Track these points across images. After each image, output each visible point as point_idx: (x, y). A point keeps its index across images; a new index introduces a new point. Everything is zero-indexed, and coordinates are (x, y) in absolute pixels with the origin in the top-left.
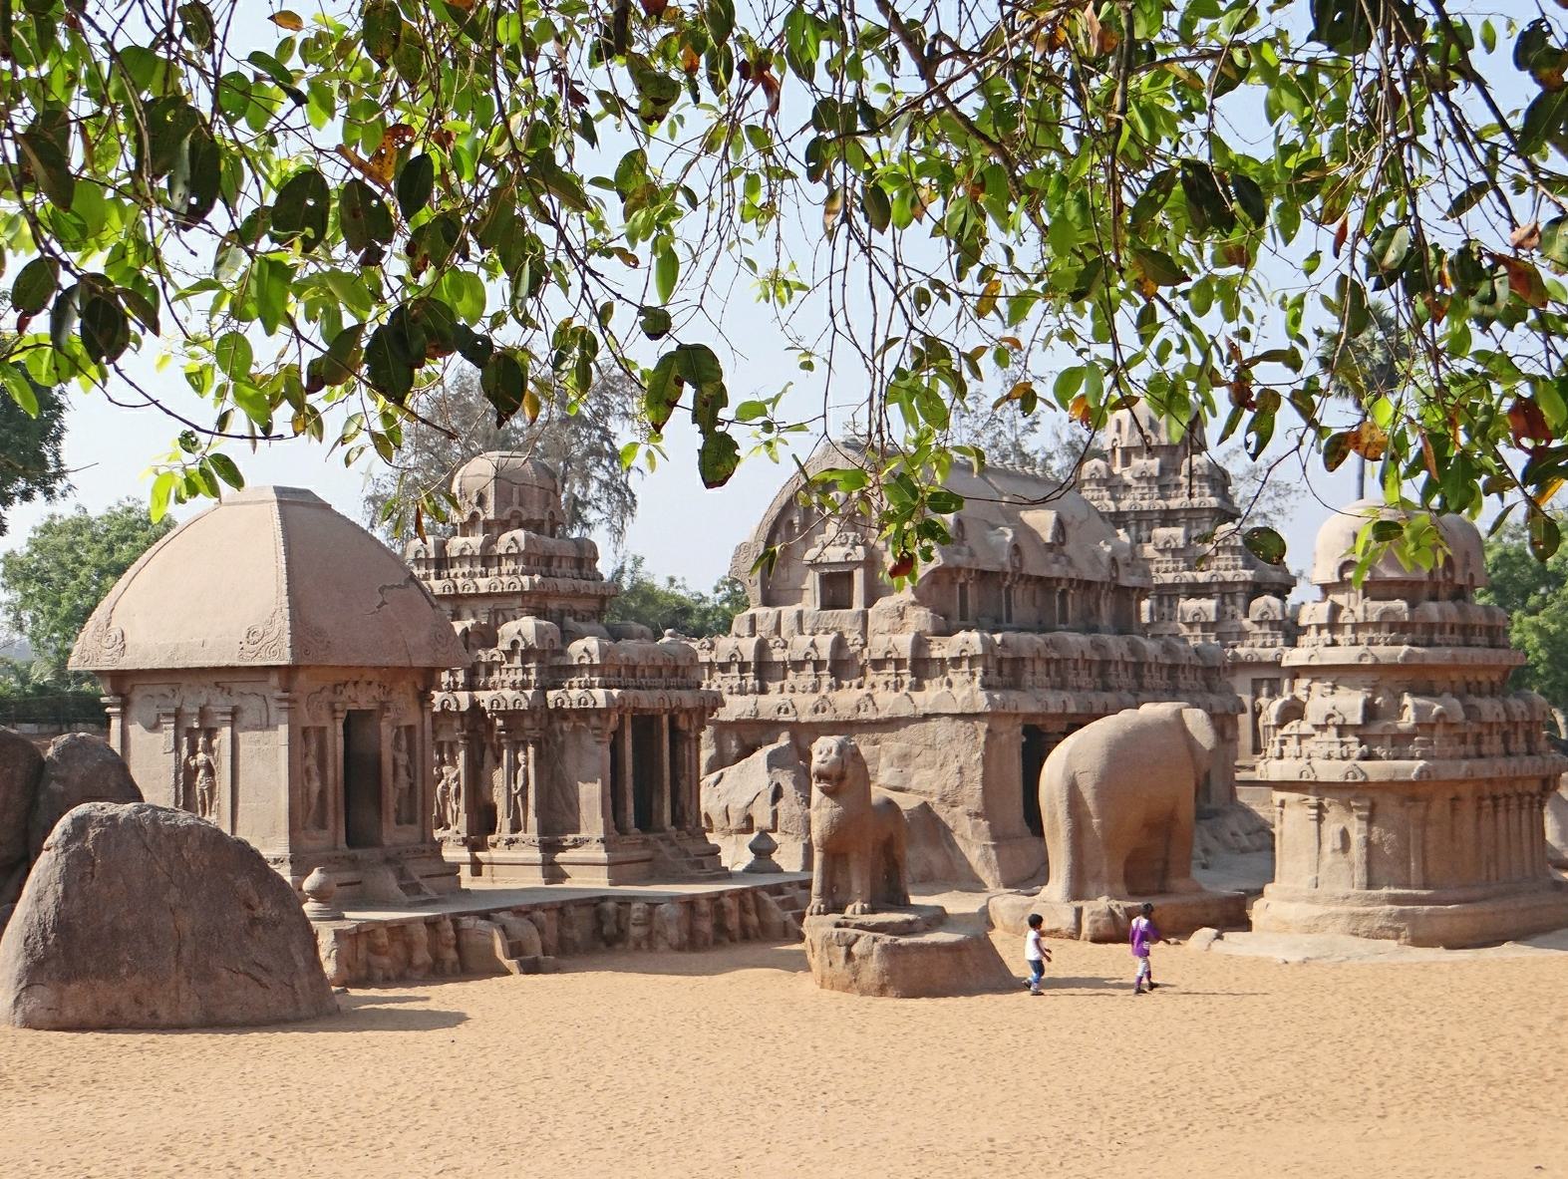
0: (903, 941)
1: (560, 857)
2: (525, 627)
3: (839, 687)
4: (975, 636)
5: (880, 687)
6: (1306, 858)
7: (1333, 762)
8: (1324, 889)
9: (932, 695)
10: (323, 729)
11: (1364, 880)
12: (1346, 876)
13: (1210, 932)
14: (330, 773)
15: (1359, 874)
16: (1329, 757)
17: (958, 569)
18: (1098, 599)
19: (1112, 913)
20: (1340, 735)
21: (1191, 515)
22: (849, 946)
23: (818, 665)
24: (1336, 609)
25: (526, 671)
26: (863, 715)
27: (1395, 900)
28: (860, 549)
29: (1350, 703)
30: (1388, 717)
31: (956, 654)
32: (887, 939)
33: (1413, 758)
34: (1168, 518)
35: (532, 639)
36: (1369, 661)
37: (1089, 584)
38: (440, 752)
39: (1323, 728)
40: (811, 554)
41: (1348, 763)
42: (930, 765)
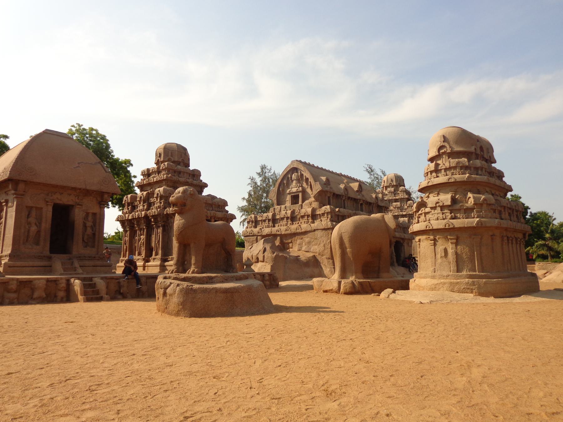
0: (196, 286)
1: (166, 263)
2: (160, 190)
3: (293, 224)
4: (328, 207)
5: (303, 223)
6: (430, 261)
7: (440, 221)
8: (437, 273)
9: (317, 224)
10: (42, 208)
11: (456, 268)
12: (447, 268)
13: (390, 290)
14: (43, 225)
15: (453, 267)
16: (438, 219)
17: (327, 191)
18: (373, 207)
19: (353, 283)
20: (441, 210)
21: (401, 200)
22: (166, 289)
23: (287, 218)
24: (437, 165)
25: (161, 203)
26: (298, 231)
27: (470, 277)
28: (301, 188)
29: (446, 198)
30: (461, 202)
31: (323, 212)
32: (185, 284)
33: (474, 218)
34: (396, 201)
35: (162, 193)
36: (453, 180)
37: (370, 203)
38: (141, 232)
39: (434, 208)
40: (288, 191)
41: (446, 221)
42: (316, 244)
